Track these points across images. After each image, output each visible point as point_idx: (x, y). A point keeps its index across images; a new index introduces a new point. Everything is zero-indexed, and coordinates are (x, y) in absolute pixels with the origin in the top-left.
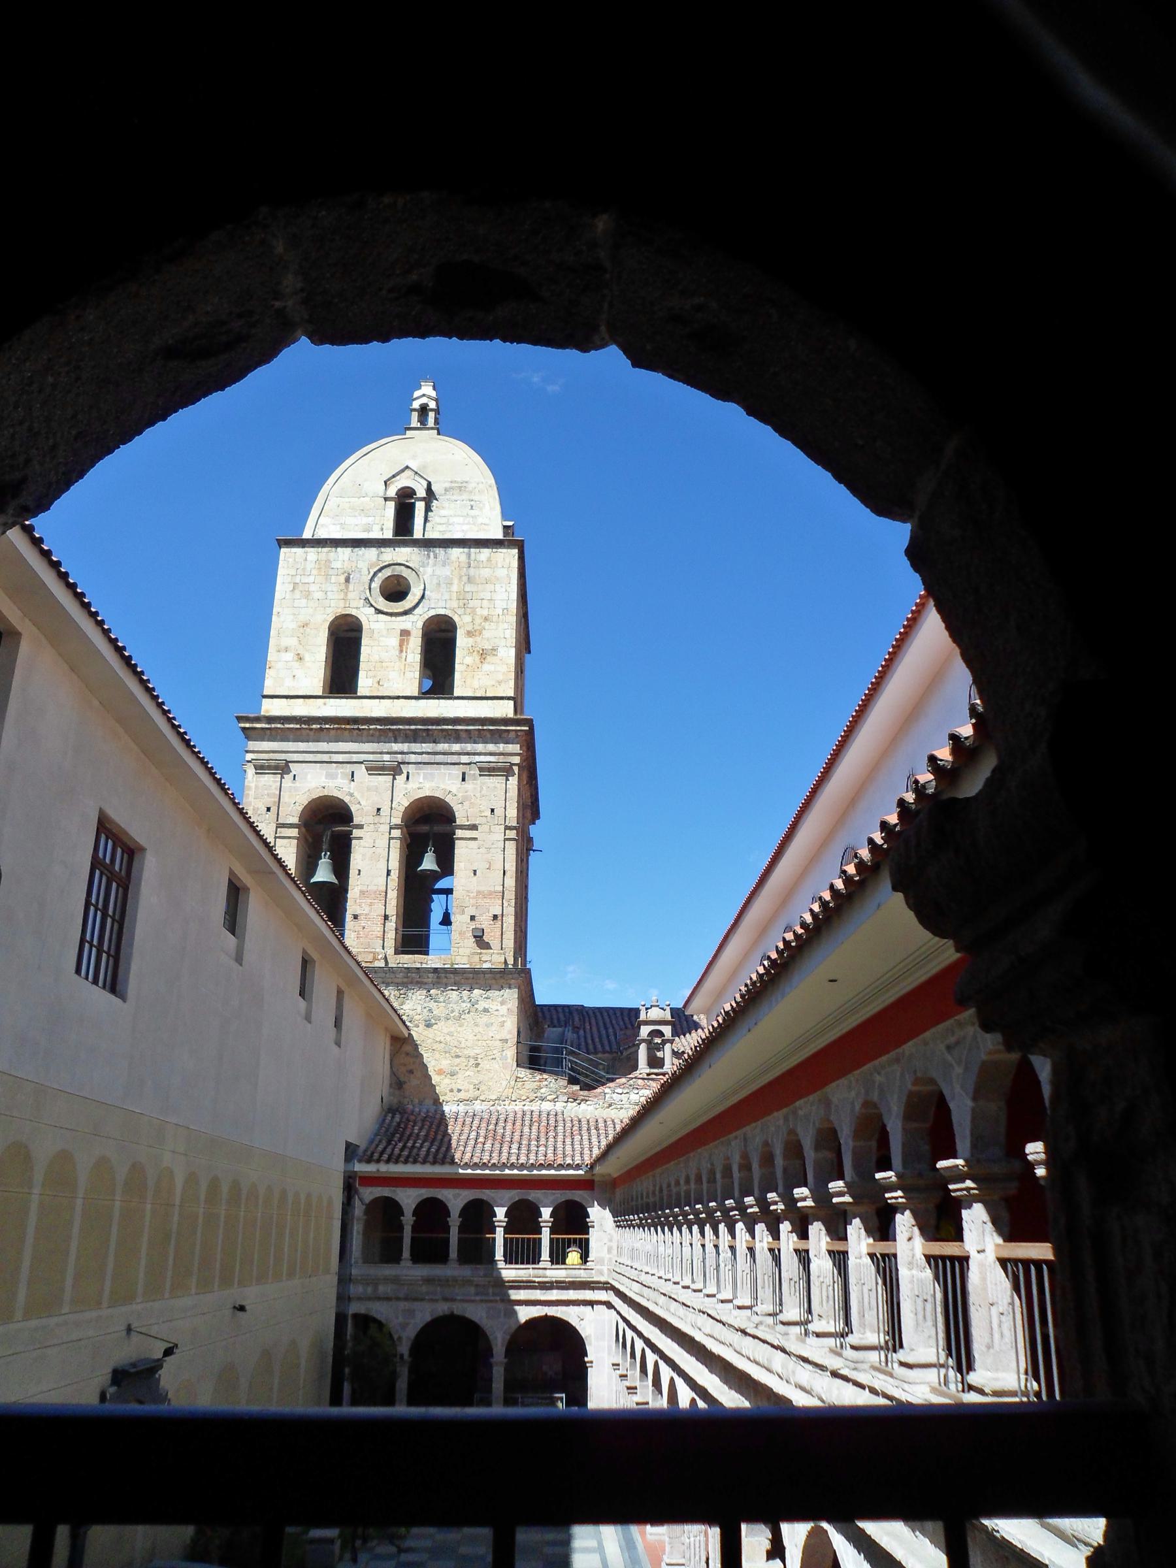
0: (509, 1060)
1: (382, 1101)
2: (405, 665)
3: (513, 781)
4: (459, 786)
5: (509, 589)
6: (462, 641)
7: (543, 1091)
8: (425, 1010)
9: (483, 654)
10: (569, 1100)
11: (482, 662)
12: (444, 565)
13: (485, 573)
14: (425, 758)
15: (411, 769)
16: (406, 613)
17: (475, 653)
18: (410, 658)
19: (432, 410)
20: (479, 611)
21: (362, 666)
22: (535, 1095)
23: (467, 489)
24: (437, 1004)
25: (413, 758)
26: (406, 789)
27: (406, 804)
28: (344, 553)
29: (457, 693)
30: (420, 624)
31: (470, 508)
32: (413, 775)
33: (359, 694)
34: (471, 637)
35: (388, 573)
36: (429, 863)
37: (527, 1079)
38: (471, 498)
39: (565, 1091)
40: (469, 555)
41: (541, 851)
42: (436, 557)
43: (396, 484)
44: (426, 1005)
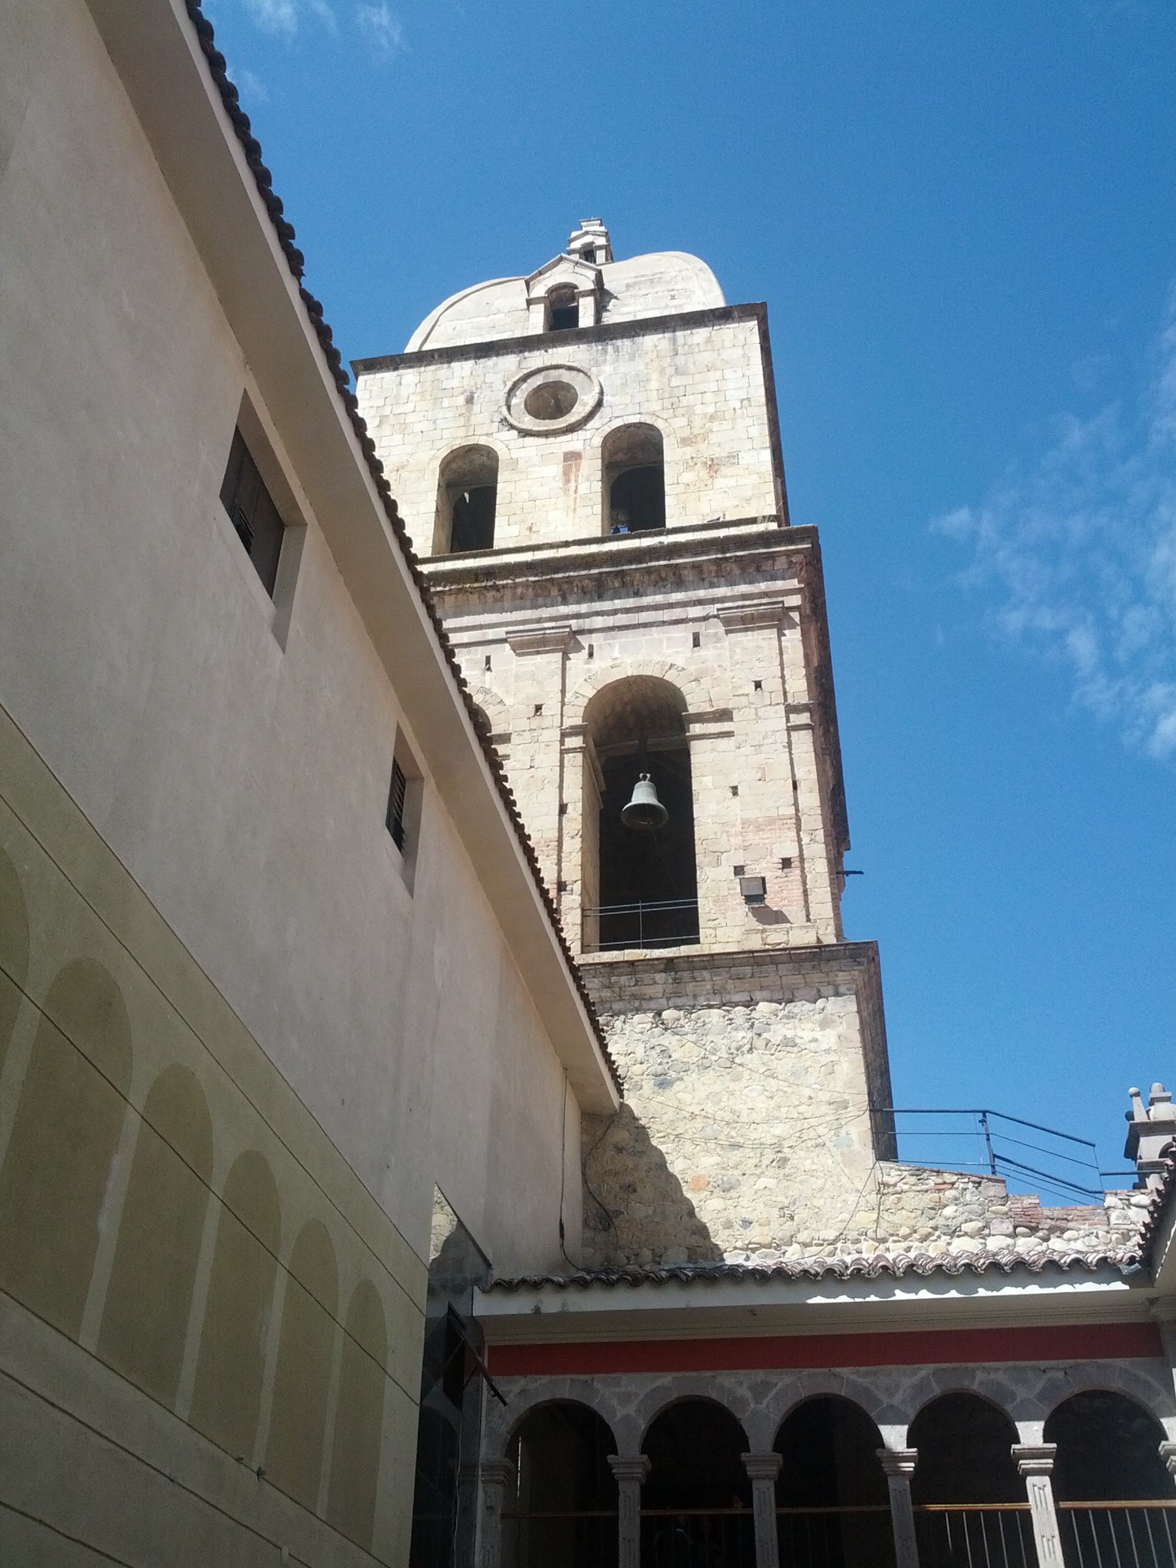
0: (857, 1146)
1: (562, 1236)
2: (575, 499)
3: (793, 637)
4: (689, 655)
5: (748, 373)
6: (672, 455)
7: (949, 1211)
8: (654, 1053)
9: (713, 466)
10: (1019, 1230)
11: (712, 477)
12: (632, 358)
13: (706, 357)
14: (622, 619)
15: (596, 639)
16: (571, 429)
17: (699, 465)
18: (583, 489)
19: (600, 248)
20: (699, 409)
21: (499, 509)
22: (932, 1224)
23: (662, 280)
24: (678, 1037)
25: (598, 622)
26: (589, 670)
27: (591, 693)
28: (463, 369)
29: (670, 524)
30: (598, 441)
31: (670, 298)
32: (600, 647)
33: (496, 547)
34: (689, 445)
35: (538, 381)
36: (642, 794)
37: (906, 1187)
38: (668, 288)
39: (1005, 1209)
40: (674, 340)
41: (861, 873)
42: (617, 350)
43: (545, 282)
44: (654, 1042)
